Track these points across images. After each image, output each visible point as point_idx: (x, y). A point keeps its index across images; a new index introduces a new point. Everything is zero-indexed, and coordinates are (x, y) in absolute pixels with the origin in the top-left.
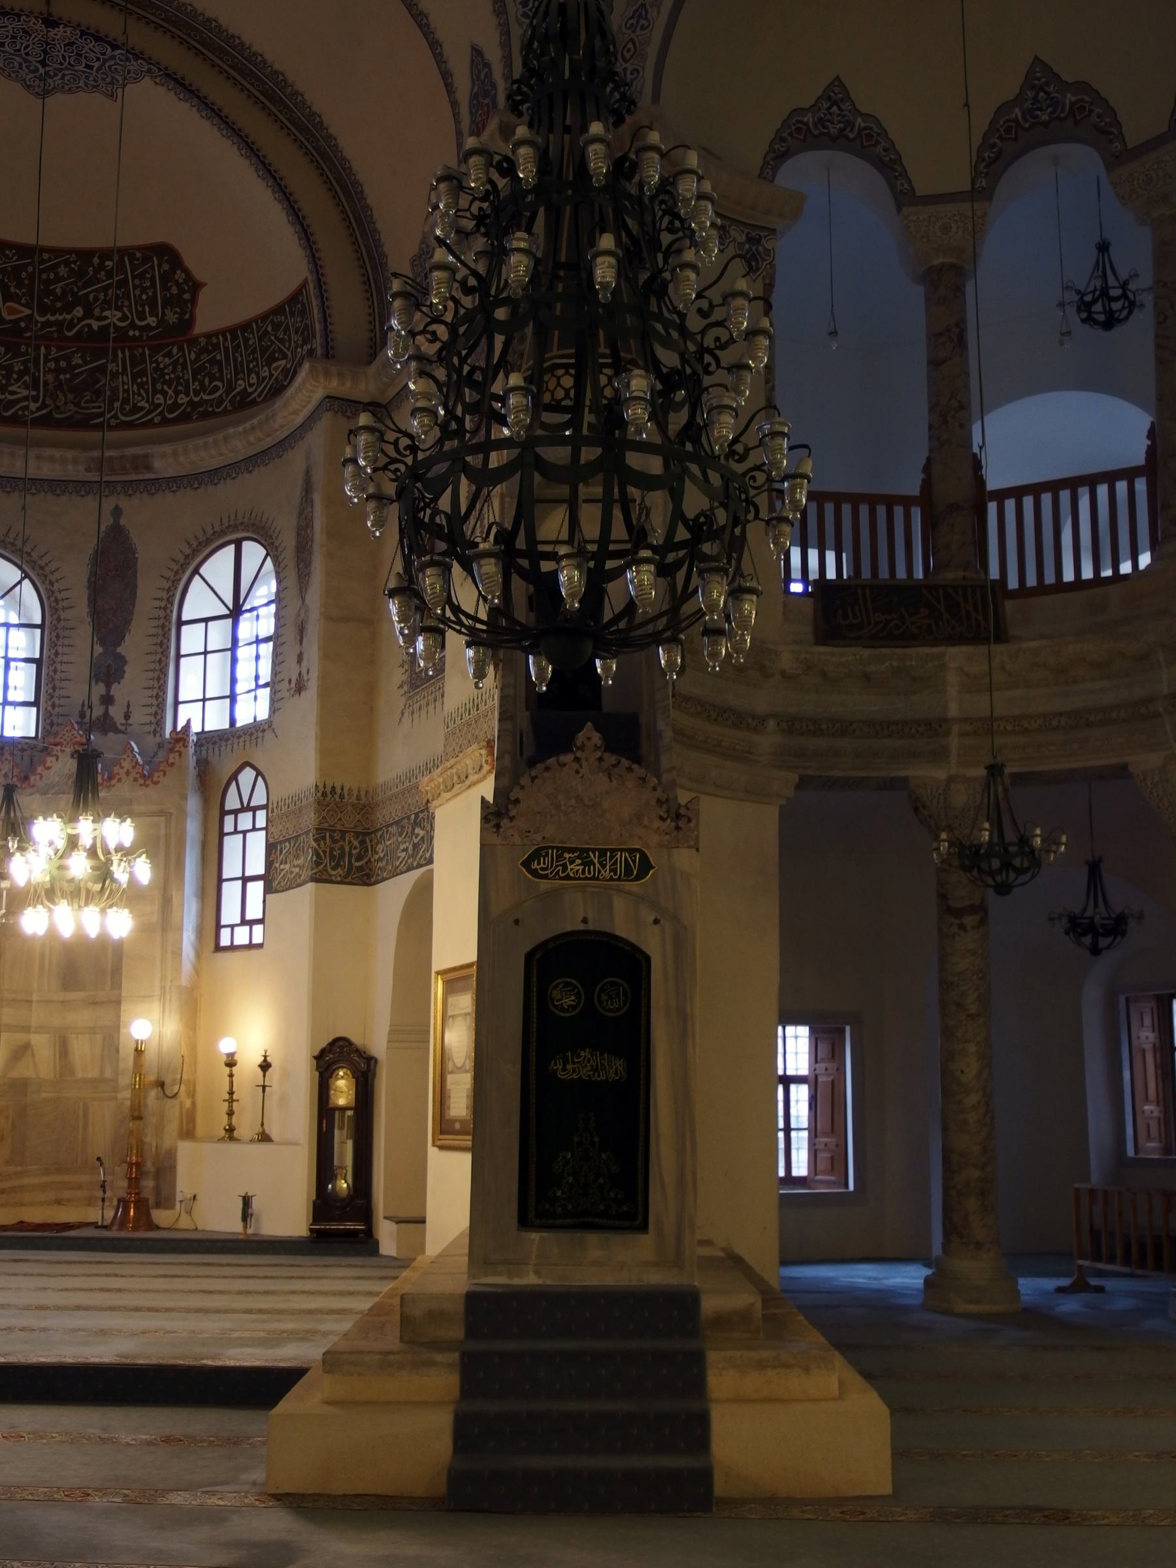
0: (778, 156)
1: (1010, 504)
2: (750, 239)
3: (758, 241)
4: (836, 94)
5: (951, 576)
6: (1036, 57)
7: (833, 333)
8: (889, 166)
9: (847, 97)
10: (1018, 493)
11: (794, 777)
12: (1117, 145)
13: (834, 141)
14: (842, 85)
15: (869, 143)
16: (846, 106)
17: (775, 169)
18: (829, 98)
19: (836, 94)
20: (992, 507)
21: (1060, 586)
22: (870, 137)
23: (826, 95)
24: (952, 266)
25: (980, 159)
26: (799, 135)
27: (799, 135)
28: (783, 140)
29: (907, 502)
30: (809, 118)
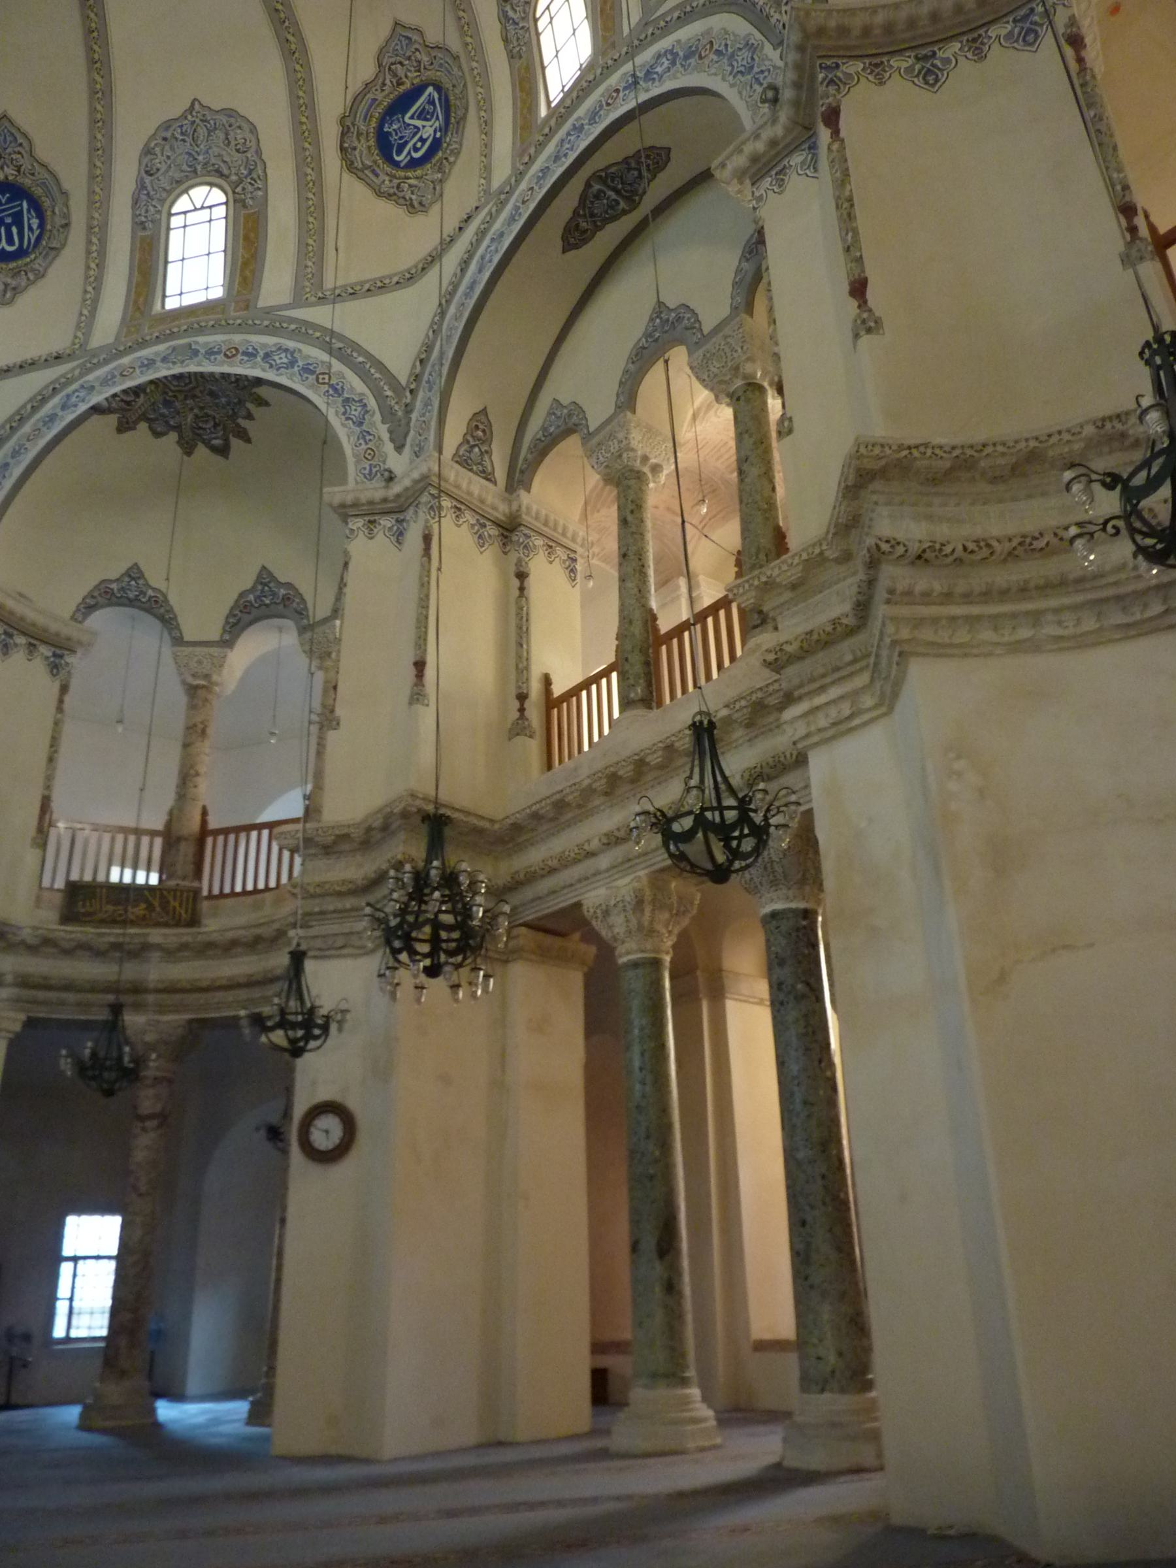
0: (88, 607)
1: (221, 838)
2: (55, 655)
3: (61, 656)
4: (134, 573)
5: (172, 883)
6: (264, 568)
7: (120, 721)
8: (167, 620)
9: (141, 575)
10: (226, 831)
11: (22, 1017)
12: (305, 621)
13: (131, 603)
14: (138, 568)
15: (157, 608)
16: (141, 582)
17: (86, 616)
18: (130, 576)
19: (134, 573)
20: (209, 841)
21: (233, 894)
22: (156, 602)
23: (128, 573)
24: (203, 687)
25: (227, 622)
26: (105, 596)
27: (105, 596)
28: (93, 597)
29: (153, 834)
30: (114, 586)
